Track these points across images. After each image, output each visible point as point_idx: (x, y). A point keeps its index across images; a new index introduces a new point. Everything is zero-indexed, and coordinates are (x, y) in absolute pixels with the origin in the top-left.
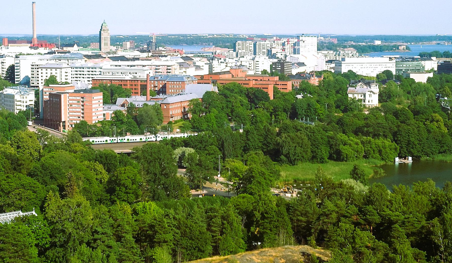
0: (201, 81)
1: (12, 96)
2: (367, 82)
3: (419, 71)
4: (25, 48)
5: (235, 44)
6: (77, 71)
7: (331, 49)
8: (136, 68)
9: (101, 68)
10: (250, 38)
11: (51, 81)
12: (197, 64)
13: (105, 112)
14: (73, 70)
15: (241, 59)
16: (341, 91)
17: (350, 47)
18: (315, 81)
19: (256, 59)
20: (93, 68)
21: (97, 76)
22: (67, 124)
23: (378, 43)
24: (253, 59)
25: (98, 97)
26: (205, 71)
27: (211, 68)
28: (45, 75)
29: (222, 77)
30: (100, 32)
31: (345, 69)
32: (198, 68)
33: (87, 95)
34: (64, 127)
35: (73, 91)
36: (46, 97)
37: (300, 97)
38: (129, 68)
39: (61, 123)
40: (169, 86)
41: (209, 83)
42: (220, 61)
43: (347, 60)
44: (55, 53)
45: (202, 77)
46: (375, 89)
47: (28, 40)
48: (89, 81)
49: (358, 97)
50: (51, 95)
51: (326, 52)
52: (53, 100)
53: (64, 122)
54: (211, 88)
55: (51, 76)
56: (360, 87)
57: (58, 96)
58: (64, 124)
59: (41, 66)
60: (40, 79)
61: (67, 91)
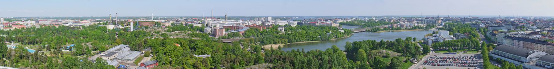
2: (282, 27)
3: (294, 24)
4: (210, 19)
10: (258, 17)
11: (215, 26)
16: (276, 29)
23: (285, 18)
25: (224, 30)
26: (248, 25)
28: (213, 25)
29: (251, 26)
31: (277, 24)
36: (214, 30)
37: (267, 30)
40: (240, 28)
43: (278, 22)
45: (247, 26)
46: (284, 28)
49: (279, 30)
50: (214, 29)
54: (248, 28)
56: (280, 28)
57: (216, 30)
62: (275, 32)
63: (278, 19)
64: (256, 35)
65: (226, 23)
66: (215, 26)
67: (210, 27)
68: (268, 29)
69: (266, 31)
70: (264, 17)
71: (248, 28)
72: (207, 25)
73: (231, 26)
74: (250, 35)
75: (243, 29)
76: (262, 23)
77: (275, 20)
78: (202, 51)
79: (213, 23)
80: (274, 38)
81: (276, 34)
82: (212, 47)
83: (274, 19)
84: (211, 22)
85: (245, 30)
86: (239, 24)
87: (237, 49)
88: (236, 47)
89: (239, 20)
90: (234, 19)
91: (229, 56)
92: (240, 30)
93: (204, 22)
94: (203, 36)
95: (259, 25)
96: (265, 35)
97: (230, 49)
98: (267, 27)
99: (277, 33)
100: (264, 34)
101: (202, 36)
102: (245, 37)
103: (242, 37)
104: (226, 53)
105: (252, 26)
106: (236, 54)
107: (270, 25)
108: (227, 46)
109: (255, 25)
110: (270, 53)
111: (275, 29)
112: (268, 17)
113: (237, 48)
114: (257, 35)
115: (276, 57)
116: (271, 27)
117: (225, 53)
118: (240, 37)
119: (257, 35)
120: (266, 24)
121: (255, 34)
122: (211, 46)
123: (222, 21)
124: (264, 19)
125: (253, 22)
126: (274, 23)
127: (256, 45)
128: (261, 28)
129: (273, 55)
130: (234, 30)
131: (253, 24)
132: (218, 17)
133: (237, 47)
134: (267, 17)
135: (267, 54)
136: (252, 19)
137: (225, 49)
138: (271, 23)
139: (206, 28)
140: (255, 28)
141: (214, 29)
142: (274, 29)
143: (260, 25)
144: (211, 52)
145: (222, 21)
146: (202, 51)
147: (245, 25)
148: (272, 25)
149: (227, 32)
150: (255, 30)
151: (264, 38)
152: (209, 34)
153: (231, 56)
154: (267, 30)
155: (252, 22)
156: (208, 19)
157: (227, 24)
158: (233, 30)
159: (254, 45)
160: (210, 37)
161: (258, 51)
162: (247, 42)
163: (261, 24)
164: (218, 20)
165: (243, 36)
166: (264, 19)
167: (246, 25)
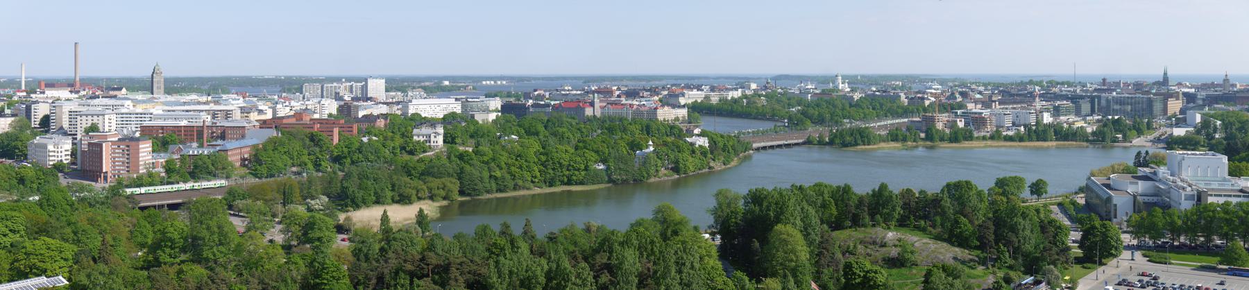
0: (264, 126)
1: (45, 146)
4: (64, 94)
5: (302, 86)
6: (123, 117)
7: (399, 91)
8: (192, 113)
9: (151, 114)
10: (317, 80)
11: (94, 128)
12: (260, 108)
13: (154, 161)
14: (118, 116)
15: (307, 103)
16: (407, 135)
17: (419, 87)
18: (381, 123)
19: (322, 103)
20: (141, 114)
21: (147, 122)
22: (109, 175)
23: (447, 83)
24: (319, 102)
26: (269, 116)
27: (275, 112)
28: (84, 123)
29: (285, 121)
30: (152, 75)
31: (411, 111)
32: (261, 112)
33: (132, 143)
34: (105, 178)
35: (117, 139)
36: (85, 148)
37: (365, 140)
38: (184, 113)
39: (102, 175)
41: (271, 128)
42: (284, 104)
43: (414, 101)
44: (99, 98)
45: (265, 122)
46: (441, 130)
47: (71, 85)
48: (137, 127)
49: (421, 139)
50: (90, 144)
51: (393, 94)
52: (93, 150)
53: (106, 172)
54: (273, 133)
55: (92, 124)
56: (425, 130)
57: (100, 146)
58: (106, 175)
59: (81, 113)
60: (79, 126)
61: (108, 140)
62: (403, 148)
63: (414, 88)
64: (310, 166)
65: (158, 110)
66: (94, 128)
67: (65, 134)
68: (369, 133)
69: (357, 145)
70: (349, 80)
71: (273, 133)
72: (46, 121)
73: (184, 123)
74: (280, 164)
75: (243, 137)
76: (340, 109)
77: (399, 93)
78: (17, 261)
79: (84, 109)
80: (395, 177)
81: (406, 157)
82: (75, 233)
83: (397, 90)
84: (67, 108)
85: (255, 141)
86: (227, 114)
87: (213, 233)
88: (208, 228)
89: (225, 97)
90: (198, 91)
91: (172, 271)
92: (230, 144)
93: (28, 109)
94: (22, 181)
95: (326, 117)
96: (353, 162)
97: (176, 236)
98: (365, 126)
99: (411, 153)
100: (349, 160)
101: (15, 182)
102: (256, 176)
103: (242, 177)
104: (157, 259)
105: (293, 121)
106: (207, 260)
107: (378, 116)
108: (158, 227)
109: (306, 119)
110: (377, 247)
111: (403, 135)
112: (370, 81)
113: (216, 229)
114: (317, 166)
115: (405, 261)
116: (381, 123)
117: (151, 258)
118: (227, 178)
119: (317, 166)
120: (361, 114)
121: (305, 158)
122: (68, 230)
123: (136, 102)
124: (351, 86)
125: (297, 105)
126: (395, 108)
127: (309, 210)
128: (336, 131)
129: (390, 254)
130: (201, 146)
131: (298, 115)
132: (109, 79)
133: (213, 224)
134: (366, 80)
135: (360, 250)
136: (289, 91)
137: (150, 242)
138: (384, 109)
139: (38, 140)
140: (308, 131)
141: (90, 144)
142: (398, 136)
143: (330, 115)
144: (70, 263)
145: (136, 102)
146: (17, 261)
147: (254, 116)
148: (385, 116)
149: (162, 159)
150: (307, 141)
151: (348, 176)
152: (59, 167)
153: (180, 272)
154: (365, 140)
155: (293, 103)
156: (51, 93)
157: (159, 117)
158: (195, 145)
159: (301, 210)
160: (63, 181)
161: (319, 239)
162: (266, 201)
163: (334, 112)
164: (115, 97)
165: (244, 171)
166: (351, 91)
167: (263, 117)
